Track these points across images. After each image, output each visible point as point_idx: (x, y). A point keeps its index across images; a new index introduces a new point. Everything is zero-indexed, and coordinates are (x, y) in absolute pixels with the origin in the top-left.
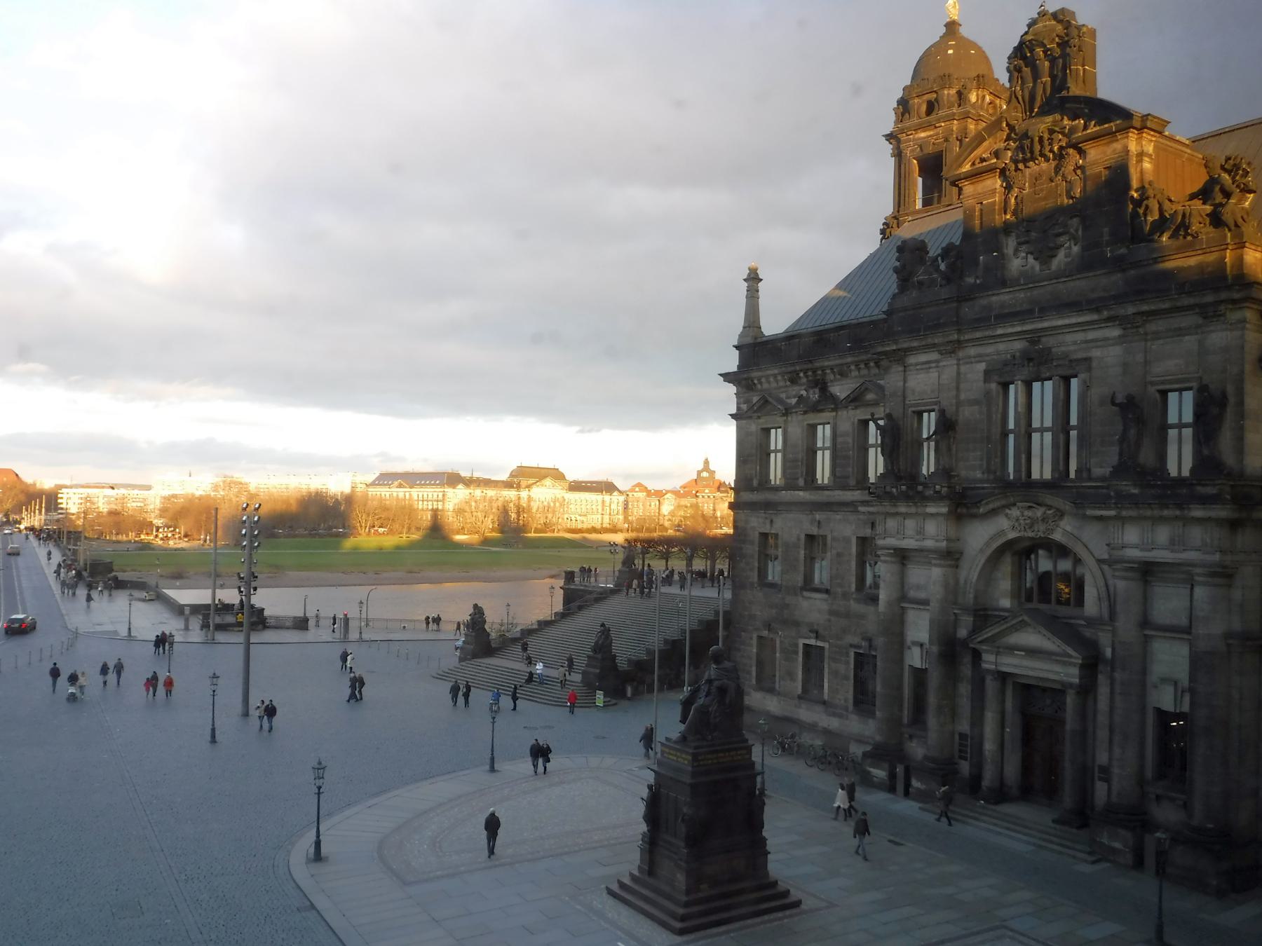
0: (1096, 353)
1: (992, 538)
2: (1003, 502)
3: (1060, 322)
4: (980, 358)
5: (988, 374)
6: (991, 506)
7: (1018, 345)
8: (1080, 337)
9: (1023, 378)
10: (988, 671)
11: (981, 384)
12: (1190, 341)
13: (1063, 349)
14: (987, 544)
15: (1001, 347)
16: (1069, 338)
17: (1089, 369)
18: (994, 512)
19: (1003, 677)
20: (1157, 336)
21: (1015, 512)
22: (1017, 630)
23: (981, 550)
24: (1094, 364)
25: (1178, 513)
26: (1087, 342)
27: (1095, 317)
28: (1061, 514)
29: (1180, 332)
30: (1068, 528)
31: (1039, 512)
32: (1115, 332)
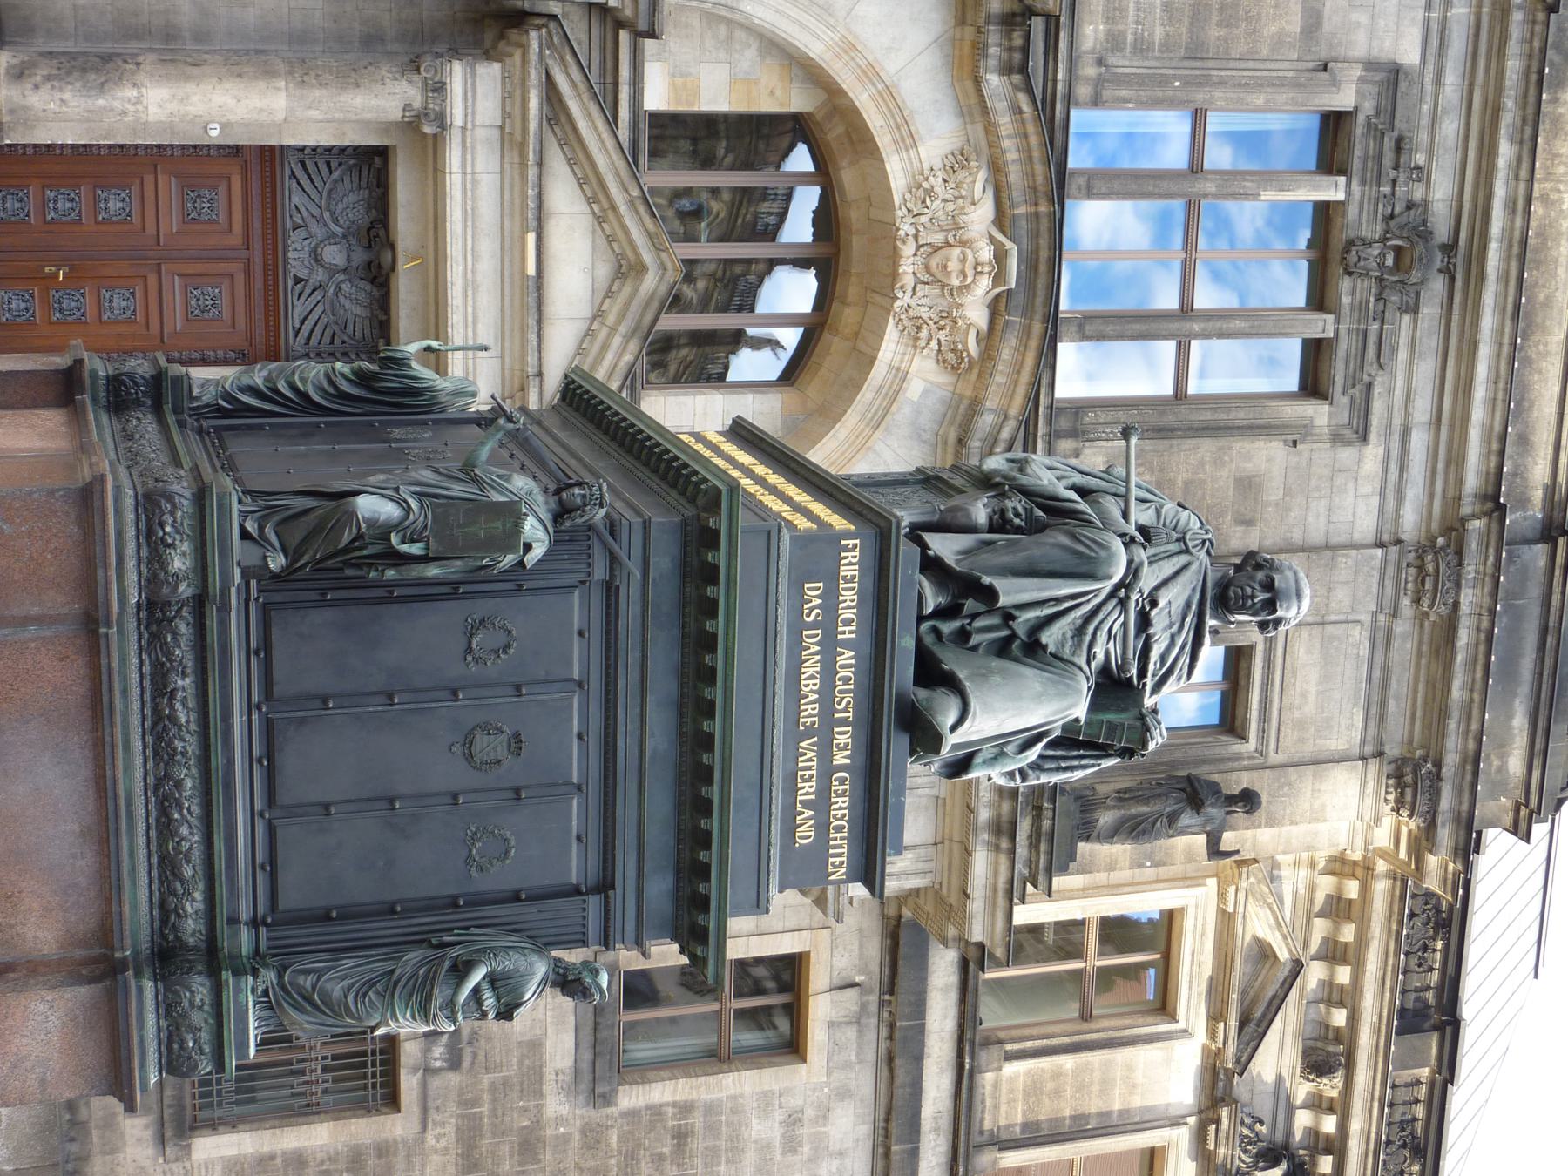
0: (1372, 455)
1: (888, 95)
2: (1015, 174)
3: (1482, 371)
4: (1435, 41)
5: (1390, 78)
6: (1005, 122)
7: (1441, 191)
8: (1422, 409)
9: (1353, 211)
10: (439, 88)
11: (1360, 46)
12: (1348, 731)
13: (1403, 355)
14: (870, 73)
15: (1450, 128)
16: (1426, 370)
17: (1337, 439)
18: (975, 108)
19: (425, 133)
20: (1381, 639)
21: (980, 216)
22: (600, 220)
23: (849, 47)
24: (1346, 455)
25: (984, 815)
26: (1406, 433)
27: (1472, 481)
28: (952, 360)
29: (1377, 698)
30: (914, 389)
31: (976, 313)
32: (1410, 521)
